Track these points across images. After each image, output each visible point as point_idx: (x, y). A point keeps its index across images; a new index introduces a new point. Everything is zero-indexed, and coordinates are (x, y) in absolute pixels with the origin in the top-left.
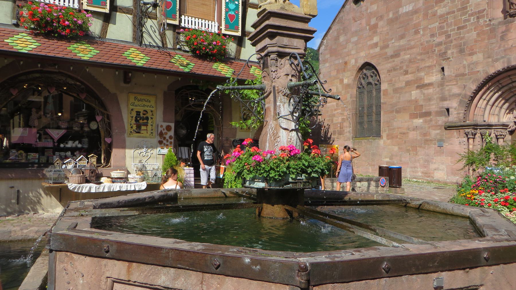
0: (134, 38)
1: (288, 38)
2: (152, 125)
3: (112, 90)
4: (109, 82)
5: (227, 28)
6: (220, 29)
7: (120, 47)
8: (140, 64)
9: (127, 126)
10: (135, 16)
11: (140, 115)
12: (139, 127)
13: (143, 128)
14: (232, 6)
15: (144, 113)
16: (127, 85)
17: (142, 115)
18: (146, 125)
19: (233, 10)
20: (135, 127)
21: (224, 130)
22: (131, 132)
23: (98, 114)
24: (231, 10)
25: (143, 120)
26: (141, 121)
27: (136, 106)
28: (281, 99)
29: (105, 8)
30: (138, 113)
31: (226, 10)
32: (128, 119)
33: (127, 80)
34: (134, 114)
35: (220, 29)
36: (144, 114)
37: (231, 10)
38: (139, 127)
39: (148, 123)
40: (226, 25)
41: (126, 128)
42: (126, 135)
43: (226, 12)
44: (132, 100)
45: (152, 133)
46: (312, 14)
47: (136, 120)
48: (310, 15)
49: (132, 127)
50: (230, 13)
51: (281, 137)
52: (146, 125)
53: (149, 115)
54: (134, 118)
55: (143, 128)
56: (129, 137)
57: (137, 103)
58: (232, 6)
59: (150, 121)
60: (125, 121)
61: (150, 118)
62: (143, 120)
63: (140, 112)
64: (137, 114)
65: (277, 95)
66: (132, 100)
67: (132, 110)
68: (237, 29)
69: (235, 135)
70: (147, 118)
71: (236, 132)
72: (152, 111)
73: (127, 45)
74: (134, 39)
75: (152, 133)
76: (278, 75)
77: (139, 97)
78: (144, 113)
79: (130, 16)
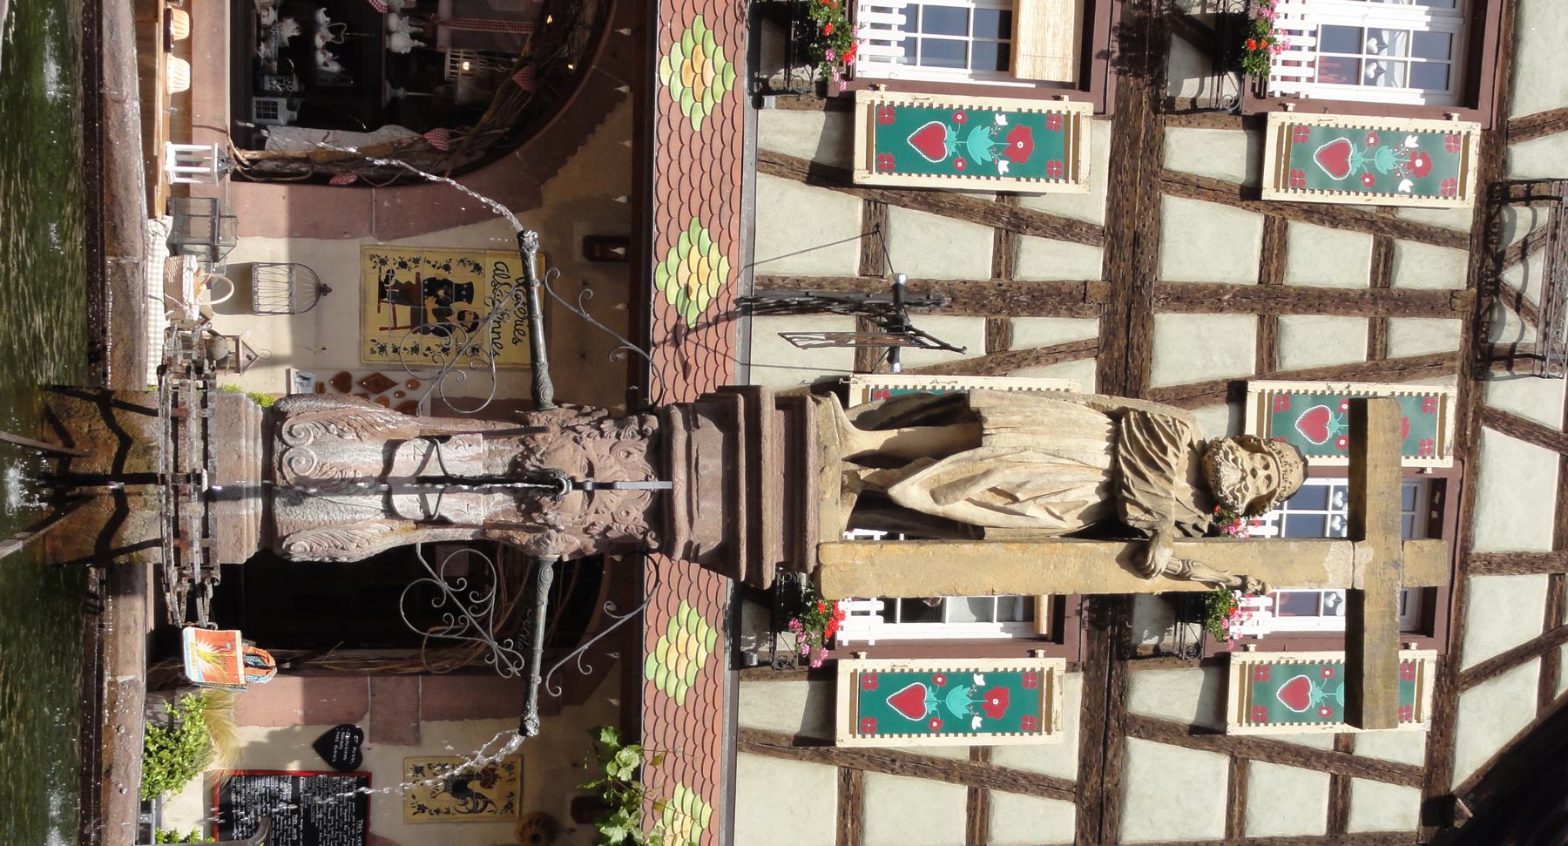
0: (770, 280)
1: (719, 474)
2: (415, 350)
3: (554, 191)
4: (587, 174)
5: (867, 684)
6: (853, 652)
7: (732, 224)
8: (660, 277)
9: (405, 246)
10: (859, 285)
11: (459, 299)
12: (405, 294)
13: (404, 313)
14: (958, 702)
15: (469, 318)
16: (577, 250)
17: (457, 306)
18: (418, 322)
19: (942, 707)
20: (404, 277)
21: (408, 680)
22: (383, 262)
23: (452, 136)
24: (941, 695)
25: (435, 312)
26: (430, 304)
27: (495, 285)
28: (501, 453)
29: (869, 167)
30: (466, 293)
31: (939, 673)
32: (434, 250)
33: (596, 248)
34: (459, 276)
35: (853, 652)
36: (461, 315)
37: (941, 695)
38: (405, 294)
39: (426, 331)
40: (874, 675)
41: (399, 242)
42: (370, 240)
43: (929, 678)
45: (382, 349)
46: (824, 573)
47: (433, 285)
48: (818, 568)
49: (403, 265)
50: (929, 694)
51: (358, 445)
52: (418, 322)
53: (459, 338)
54: (442, 274)
55: (404, 313)
56: (362, 252)
58: (958, 702)
59: (431, 340)
60: (430, 239)
61: (443, 341)
62: (435, 312)
63: (470, 301)
64: (459, 287)
65: (515, 439)
67: (478, 268)
68: (864, 724)
69: (385, 735)
71: (400, 741)
72: (475, 350)
73: (738, 251)
74: (768, 283)
75: (382, 349)
76: (589, 443)
78: (469, 318)
79: (854, 269)
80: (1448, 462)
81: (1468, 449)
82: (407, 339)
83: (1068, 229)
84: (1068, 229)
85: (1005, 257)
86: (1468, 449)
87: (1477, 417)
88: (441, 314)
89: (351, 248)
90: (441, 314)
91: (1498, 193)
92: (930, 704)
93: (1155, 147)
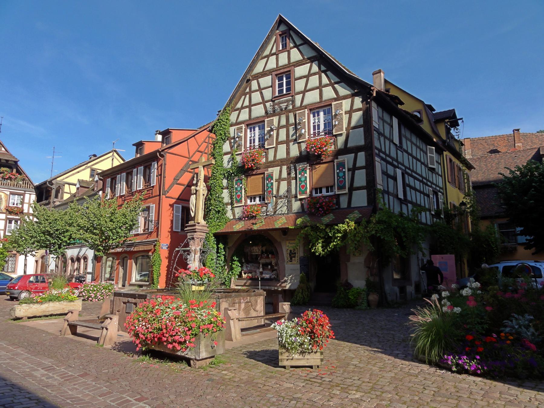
3: (279, 240)
13: (293, 259)
14: (341, 174)
30: (291, 251)
34: (289, 252)
37: (340, 177)
43: (338, 180)
44: (288, 244)
47: (290, 255)
52: (295, 257)
53: (296, 251)
55: (293, 259)
57: (290, 245)
60: (285, 255)
66: (288, 244)
70: (295, 253)
77: (291, 242)
80: (306, 110)
81: (305, 107)
82: (296, 258)
83: (281, 172)
84: (281, 172)
85: (284, 180)
86: (305, 107)
87: (302, 107)
88: (293, 254)
89: (286, 265)
90: (293, 254)
91: (274, 114)
92: (341, 179)
93: (271, 162)
